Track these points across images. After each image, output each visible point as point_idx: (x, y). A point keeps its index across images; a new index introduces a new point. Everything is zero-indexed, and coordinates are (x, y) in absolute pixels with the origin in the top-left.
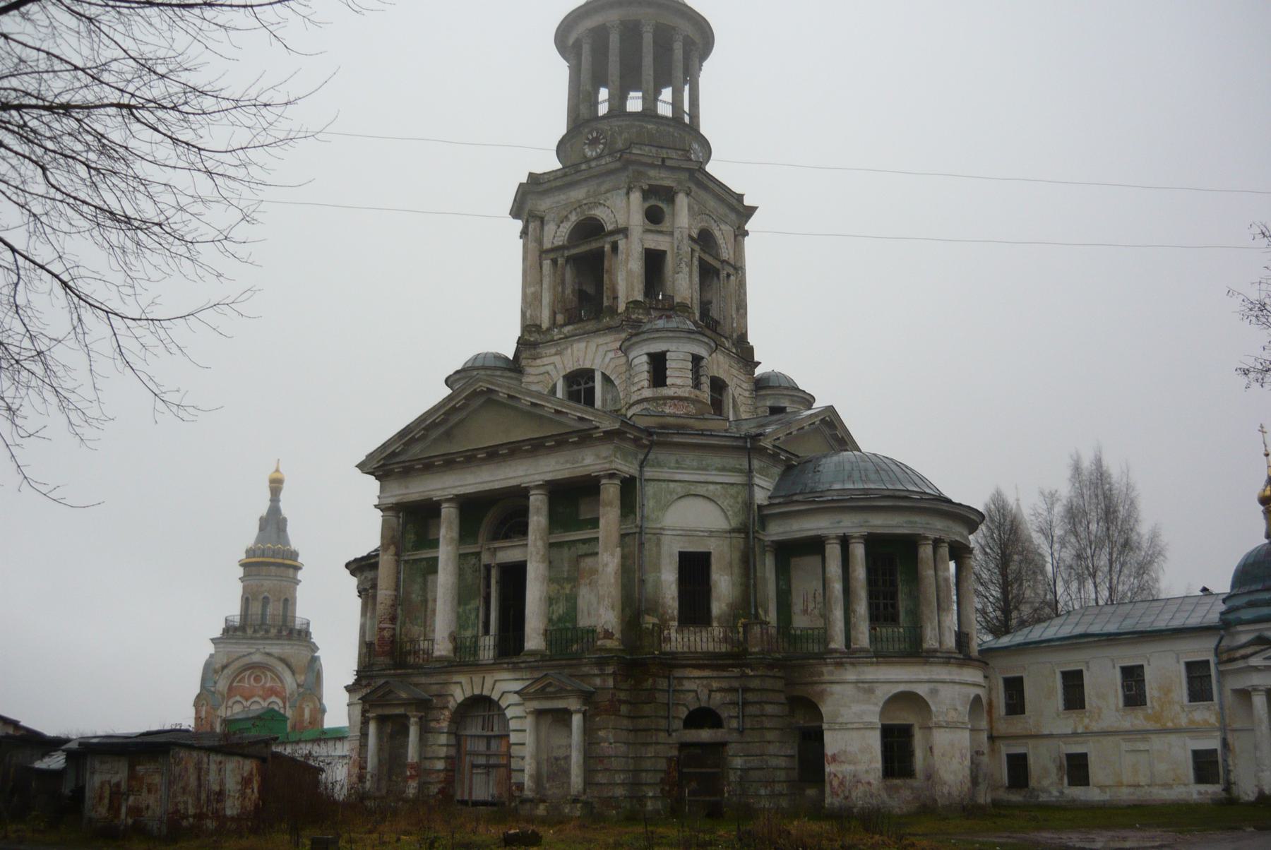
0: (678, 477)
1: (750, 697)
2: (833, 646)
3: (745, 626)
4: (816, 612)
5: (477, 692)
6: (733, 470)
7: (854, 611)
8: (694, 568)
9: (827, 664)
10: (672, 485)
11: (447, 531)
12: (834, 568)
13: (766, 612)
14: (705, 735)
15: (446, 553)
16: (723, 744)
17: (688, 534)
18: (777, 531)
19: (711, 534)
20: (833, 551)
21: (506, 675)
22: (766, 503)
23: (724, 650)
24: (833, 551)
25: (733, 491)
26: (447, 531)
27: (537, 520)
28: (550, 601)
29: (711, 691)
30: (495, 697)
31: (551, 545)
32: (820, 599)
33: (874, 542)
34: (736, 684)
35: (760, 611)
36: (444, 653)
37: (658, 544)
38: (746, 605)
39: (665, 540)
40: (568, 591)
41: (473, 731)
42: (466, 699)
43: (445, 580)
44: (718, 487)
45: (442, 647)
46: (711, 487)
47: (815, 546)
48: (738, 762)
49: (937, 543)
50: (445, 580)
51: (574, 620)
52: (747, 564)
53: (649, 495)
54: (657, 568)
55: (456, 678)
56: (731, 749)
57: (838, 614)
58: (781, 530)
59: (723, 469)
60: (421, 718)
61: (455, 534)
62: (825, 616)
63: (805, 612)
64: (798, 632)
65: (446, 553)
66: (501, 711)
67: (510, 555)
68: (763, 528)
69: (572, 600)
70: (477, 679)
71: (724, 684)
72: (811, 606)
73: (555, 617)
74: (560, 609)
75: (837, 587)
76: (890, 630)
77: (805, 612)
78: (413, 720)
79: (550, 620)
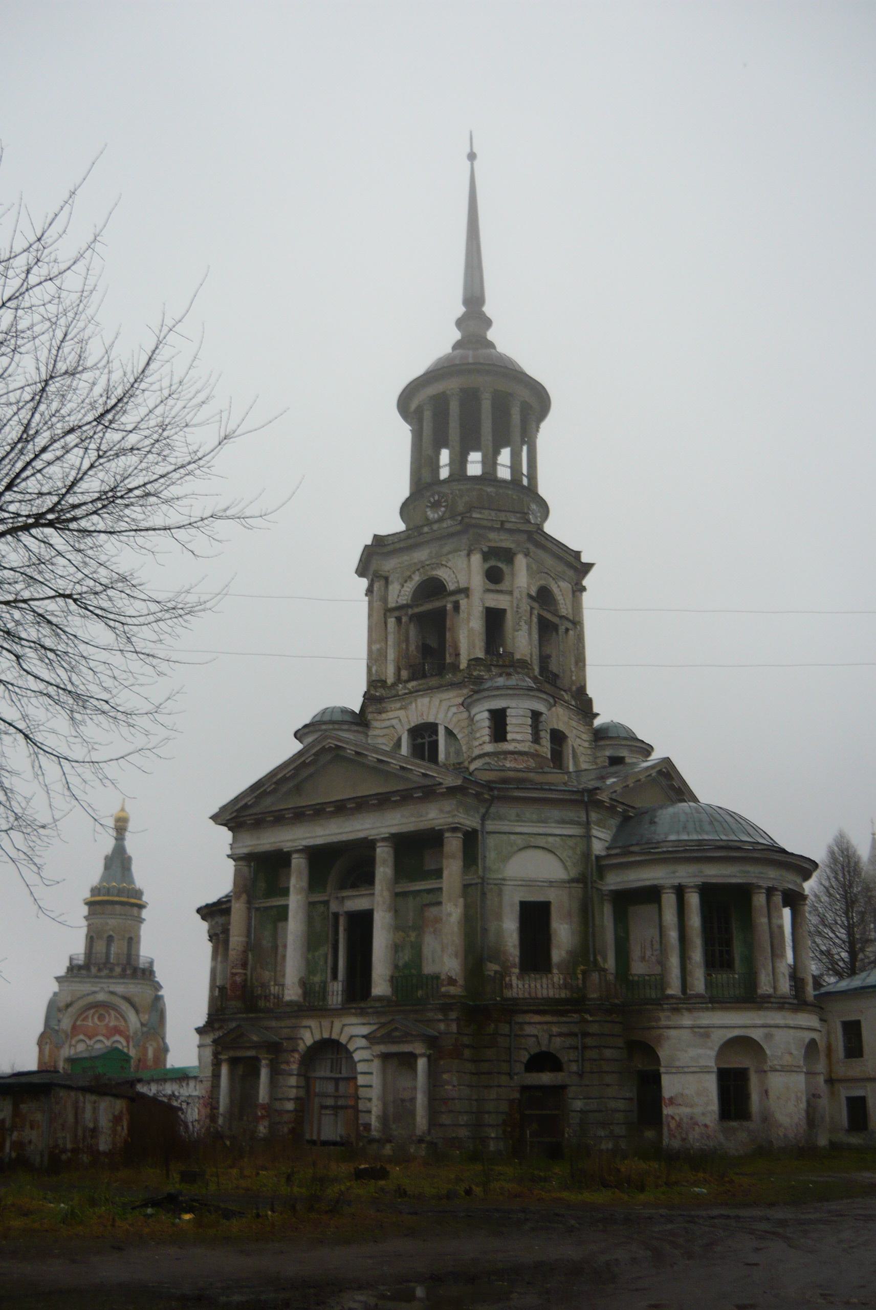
0: (518, 830)
1: (589, 1041)
2: (670, 992)
3: (584, 973)
4: (654, 959)
5: (326, 1036)
6: (572, 822)
7: (690, 958)
8: (535, 917)
9: (663, 1010)
10: (513, 837)
11: (297, 881)
12: (670, 916)
13: (605, 959)
14: (546, 1078)
15: (295, 902)
16: (563, 1087)
17: (529, 884)
18: (614, 881)
19: (551, 883)
20: (669, 901)
21: (354, 1020)
22: (603, 853)
23: (563, 995)
24: (669, 901)
25: (571, 842)
26: (297, 881)
27: (384, 871)
28: (396, 948)
29: (551, 1036)
30: (343, 1040)
31: (397, 895)
32: (657, 946)
33: (707, 891)
34: (575, 1029)
35: (599, 959)
36: (294, 998)
37: (500, 894)
38: (585, 953)
39: (507, 891)
40: (413, 939)
41: (322, 1074)
42: (315, 1043)
43: (295, 927)
44: (557, 839)
45: (292, 992)
46: (550, 839)
47: (652, 894)
48: (578, 1104)
49: (770, 891)
50: (295, 927)
51: (419, 966)
52: (586, 915)
53: (491, 847)
54: (499, 917)
55: (306, 1022)
56: (571, 1092)
57: (674, 961)
58: (619, 880)
59: (563, 822)
60: (271, 1061)
61: (304, 883)
62: (662, 962)
63: (643, 959)
64: (636, 978)
65: (295, 902)
66: (349, 1054)
67: (357, 904)
68: (601, 877)
69: (417, 949)
70: (326, 1023)
71: (564, 1029)
72: (648, 953)
73: (401, 964)
74: (406, 956)
75: (673, 935)
76: (724, 976)
77: (643, 959)
78: (264, 1062)
79: (396, 967)
